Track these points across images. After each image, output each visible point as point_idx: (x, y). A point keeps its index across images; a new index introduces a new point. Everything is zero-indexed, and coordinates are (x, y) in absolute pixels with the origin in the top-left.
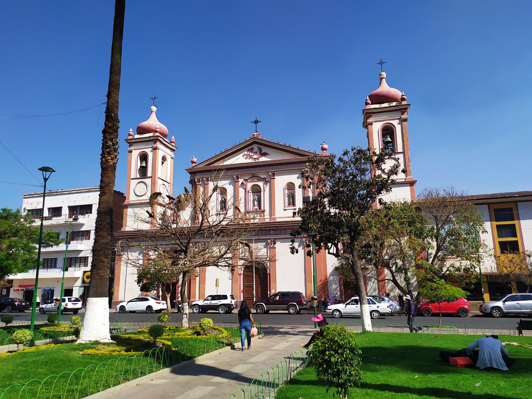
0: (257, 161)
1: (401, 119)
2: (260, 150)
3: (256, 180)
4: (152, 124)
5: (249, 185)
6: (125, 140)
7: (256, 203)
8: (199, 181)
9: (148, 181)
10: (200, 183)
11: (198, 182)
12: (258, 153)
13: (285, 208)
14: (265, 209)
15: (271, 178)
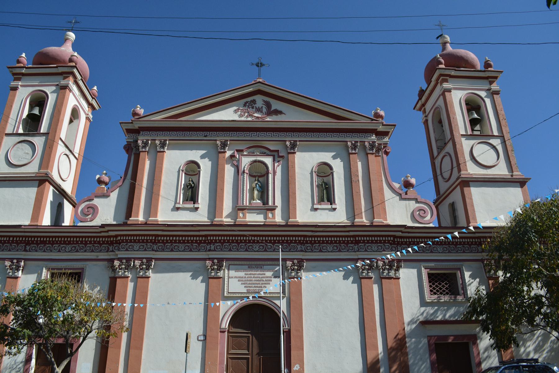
0: (260, 120)
1: (491, 91)
2: (268, 105)
3: (258, 154)
4: (65, 50)
5: (246, 161)
6: (9, 68)
7: (256, 192)
8: (145, 144)
9: (39, 141)
10: (147, 149)
11: (143, 147)
12: (264, 110)
13: (315, 207)
14: (276, 204)
15: (289, 151)
